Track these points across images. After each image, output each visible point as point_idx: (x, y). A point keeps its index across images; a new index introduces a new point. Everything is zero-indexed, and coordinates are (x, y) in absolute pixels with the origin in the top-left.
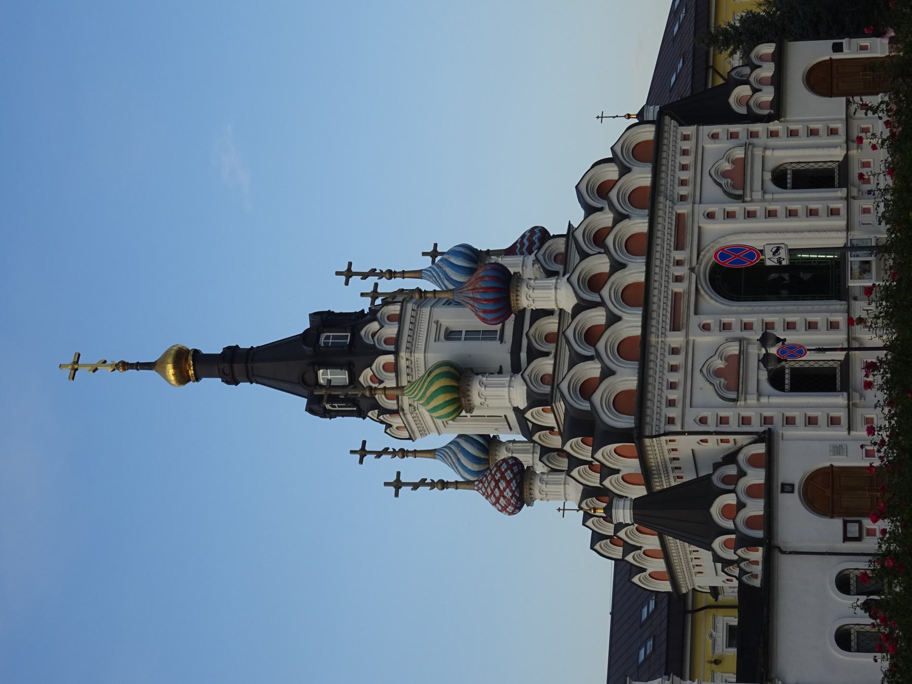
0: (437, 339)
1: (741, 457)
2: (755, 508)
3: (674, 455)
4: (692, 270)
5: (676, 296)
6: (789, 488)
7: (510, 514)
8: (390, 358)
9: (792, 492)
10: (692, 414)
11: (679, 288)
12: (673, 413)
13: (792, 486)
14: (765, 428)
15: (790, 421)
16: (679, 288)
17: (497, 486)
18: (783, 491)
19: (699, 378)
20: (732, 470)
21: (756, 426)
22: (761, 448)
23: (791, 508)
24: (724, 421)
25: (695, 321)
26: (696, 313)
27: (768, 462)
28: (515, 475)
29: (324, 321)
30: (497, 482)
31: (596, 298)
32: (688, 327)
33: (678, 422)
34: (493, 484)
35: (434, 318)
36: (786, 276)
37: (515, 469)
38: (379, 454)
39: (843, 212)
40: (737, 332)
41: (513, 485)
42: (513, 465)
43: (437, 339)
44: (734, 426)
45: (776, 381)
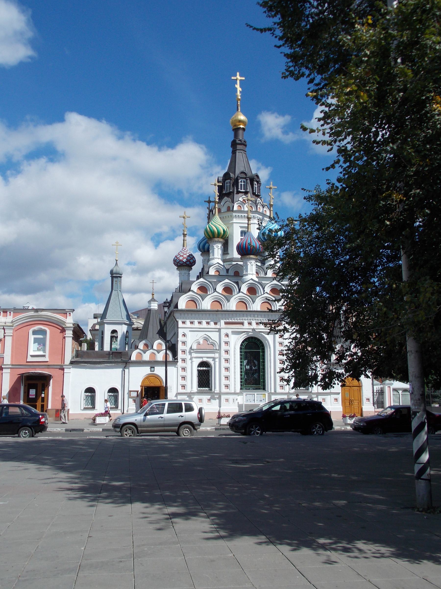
2: (146, 357)
4: (254, 330)
5: (242, 324)
6: (152, 369)
9: (151, 371)
10: (186, 331)
11: (246, 325)
13: (154, 371)
14: (180, 360)
15: (184, 369)
16: (246, 325)
17: (181, 256)
18: (151, 367)
23: (146, 370)
24: (184, 343)
25: (229, 332)
26: (232, 331)
28: (185, 263)
30: (182, 256)
32: (226, 328)
33: (184, 326)
34: (182, 254)
36: (256, 368)
37: (188, 263)
38: (208, 208)
39: (282, 391)
42: (190, 262)
44: (180, 347)
45: (203, 364)
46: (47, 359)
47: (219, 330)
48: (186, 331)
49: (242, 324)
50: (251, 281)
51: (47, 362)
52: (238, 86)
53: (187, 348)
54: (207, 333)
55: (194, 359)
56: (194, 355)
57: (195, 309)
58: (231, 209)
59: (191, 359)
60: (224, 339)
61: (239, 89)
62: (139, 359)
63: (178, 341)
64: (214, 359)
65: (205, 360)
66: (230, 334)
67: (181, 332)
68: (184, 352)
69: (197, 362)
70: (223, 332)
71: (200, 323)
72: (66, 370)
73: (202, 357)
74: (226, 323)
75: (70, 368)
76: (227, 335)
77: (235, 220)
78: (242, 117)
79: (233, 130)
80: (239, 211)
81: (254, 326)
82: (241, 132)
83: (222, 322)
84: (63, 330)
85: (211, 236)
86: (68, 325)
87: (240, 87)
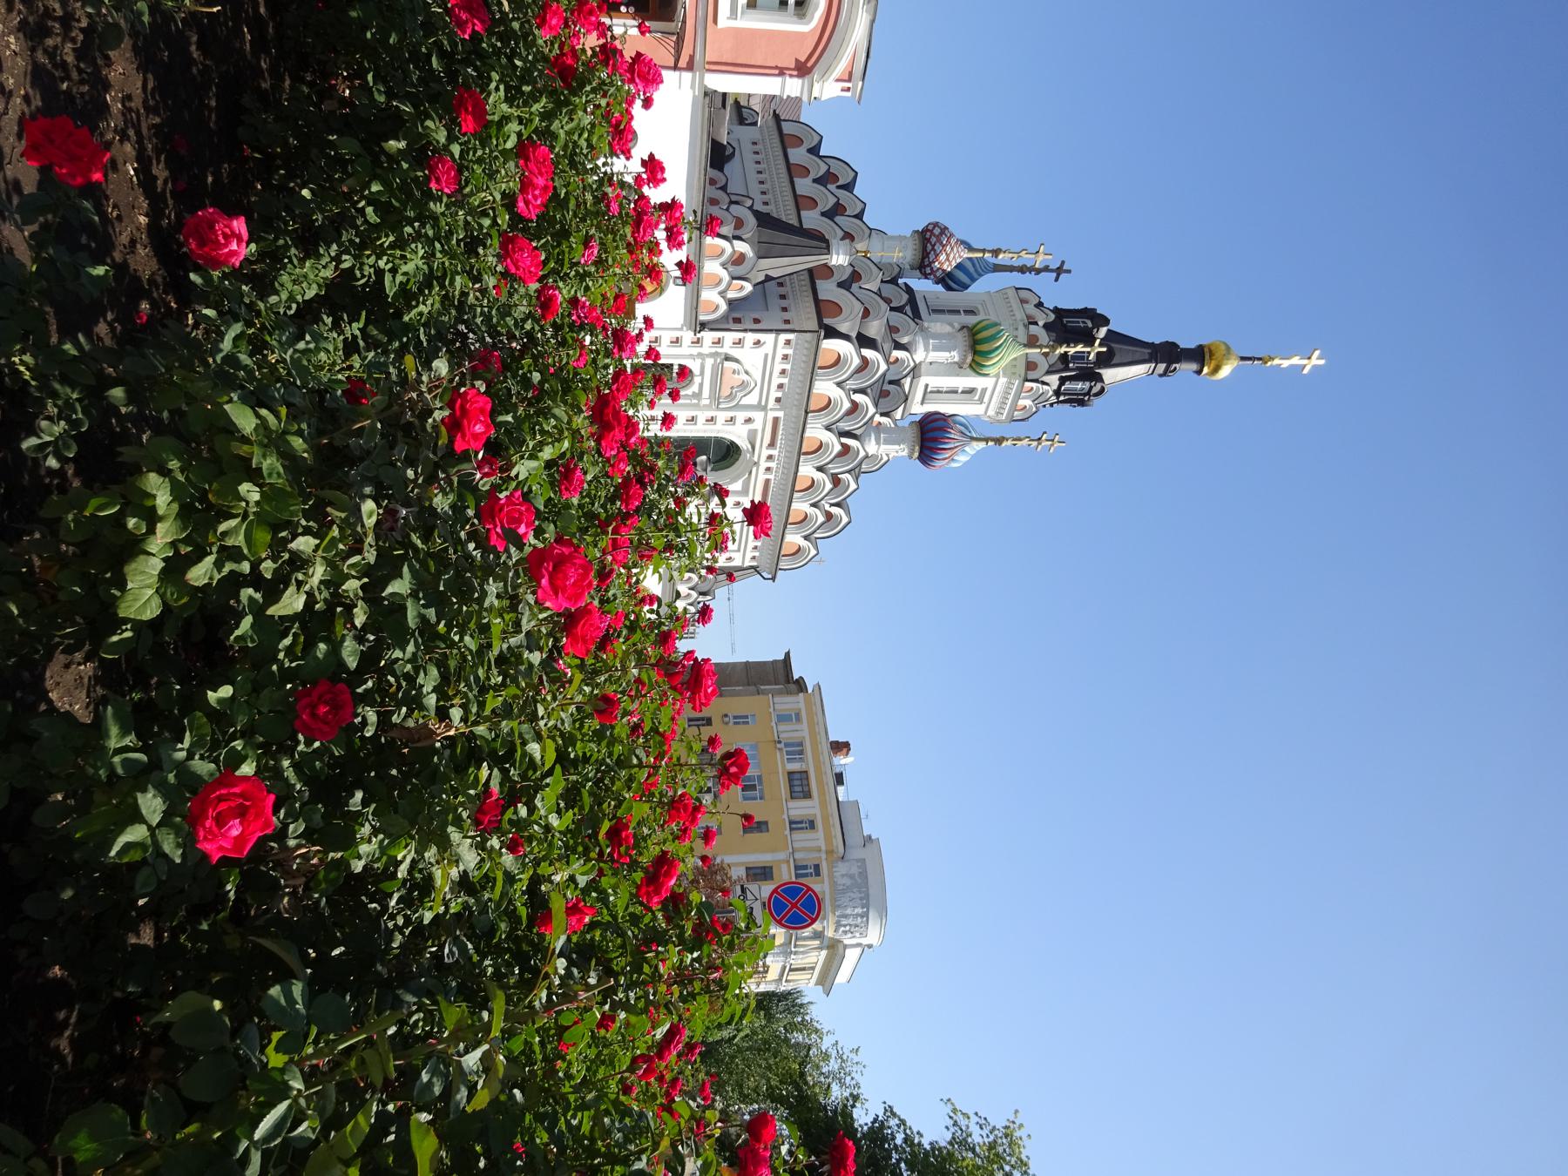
0: (984, 390)
1: (724, 307)
3: (784, 303)
7: (936, 225)
8: (1031, 375)
12: (781, 351)
19: (757, 375)
20: (731, 295)
21: (708, 336)
22: (702, 318)
24: (739, 342)
25: (757, 425)
27: (694, 304)
29: (1079, 400)
31: (844, 440)
35: (984, 406)
40: (722, 416)
41: (932, 256)
43: (984, 390)
44: (730, 337)
46: (724, 21)
47: (764, 408)
48: (768, 348)
49: (772, 445)
50: (862, 454)
51: (715, 21)
52: (1296, 361)
53: (727, 348)
54: (757, 390)
55: (699, 361)
56: (709, 362)
57: (819, 364)
58: (1031, 375)
59: (700, 355)
60: (741, 416)
61: (1285, 363)
62: (706, 251)
63: (745, 331)
64: (698, 395)
65: (697, 380)
66: (750, 426)
67: (768, 338)
68: (719, 342)
69: (694, 366)
70: (758, 416)
71: (783, 372)
72: (687, 76)
73: (702, 374)
74: (776, 420)
75: (693, 87)
76: (749, 421)
77: (1003, 380)
78: (1225, 371)
79: (1201, 348)
80: (1021, 389)
81: (764, 465)
82: (1194, 366)
83: (780, 414)
84: (802, 70)
85: (979, 348)
86: (816, 87)
87: (1292, 366)
